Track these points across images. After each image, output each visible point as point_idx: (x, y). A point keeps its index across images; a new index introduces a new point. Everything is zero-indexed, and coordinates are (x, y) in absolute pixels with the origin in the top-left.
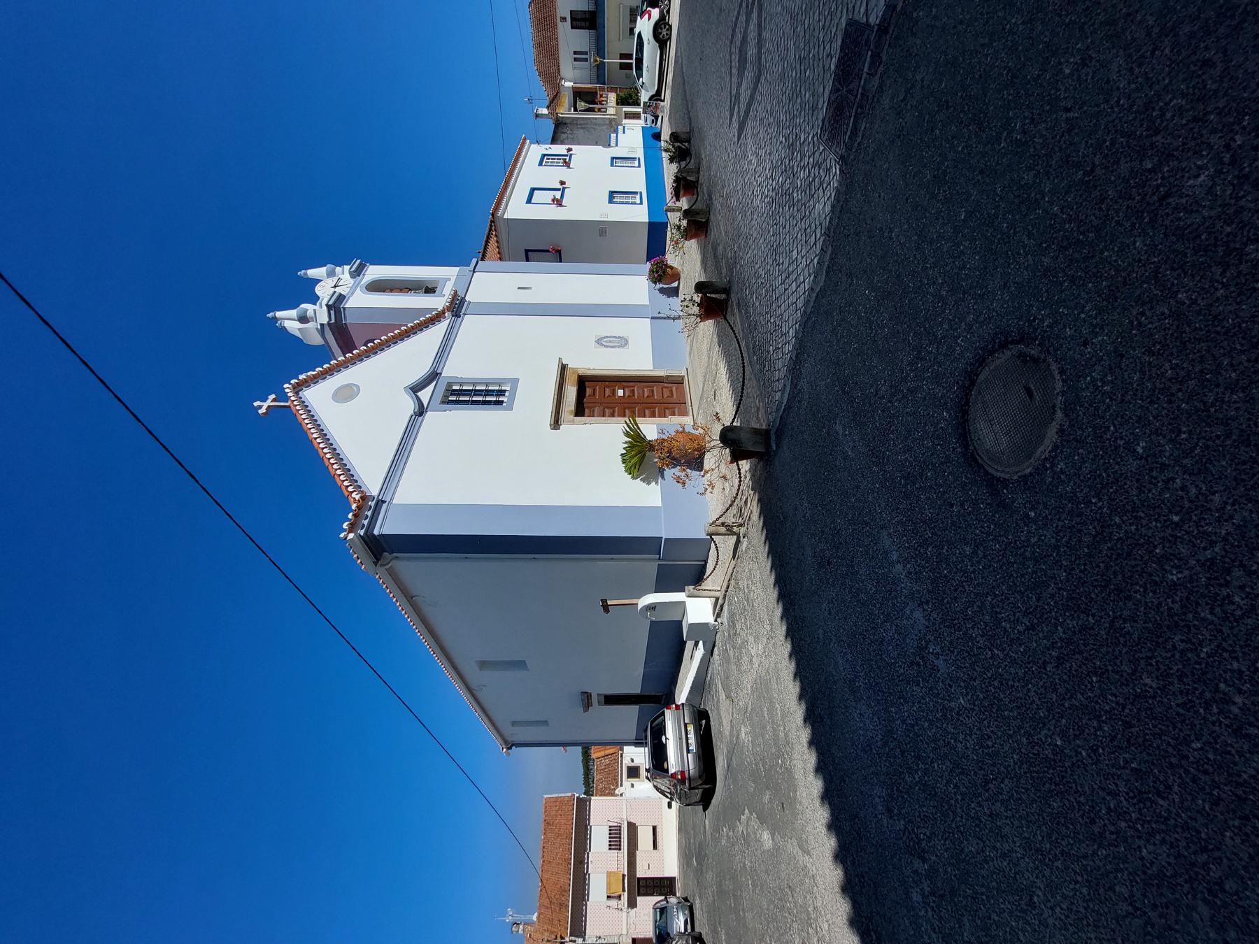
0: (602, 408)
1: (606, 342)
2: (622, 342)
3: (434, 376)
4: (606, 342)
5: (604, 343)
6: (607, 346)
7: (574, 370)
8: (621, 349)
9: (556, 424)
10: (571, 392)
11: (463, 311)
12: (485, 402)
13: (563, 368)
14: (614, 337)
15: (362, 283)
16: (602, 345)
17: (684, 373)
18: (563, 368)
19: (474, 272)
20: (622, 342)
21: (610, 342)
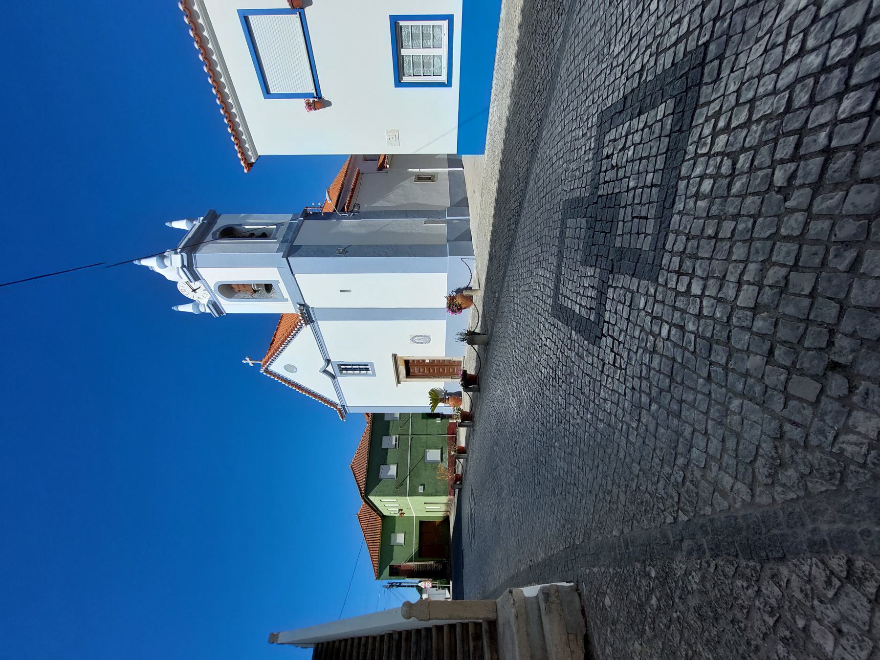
2: (427, 339)
3: (328, 361)
6: (418, 343)
7: (401, 358)
8: (427, 344)
9: (399, 382)
10: (402, 369)
11: (314, 319)
12: (359, 365)
13: (395, 356)
14: (422, 336)
15: (213, 290)
16: (414, 342)
17: (462, 359)
18: (395, 356)
20: (427, 339)
21: (420, 339)
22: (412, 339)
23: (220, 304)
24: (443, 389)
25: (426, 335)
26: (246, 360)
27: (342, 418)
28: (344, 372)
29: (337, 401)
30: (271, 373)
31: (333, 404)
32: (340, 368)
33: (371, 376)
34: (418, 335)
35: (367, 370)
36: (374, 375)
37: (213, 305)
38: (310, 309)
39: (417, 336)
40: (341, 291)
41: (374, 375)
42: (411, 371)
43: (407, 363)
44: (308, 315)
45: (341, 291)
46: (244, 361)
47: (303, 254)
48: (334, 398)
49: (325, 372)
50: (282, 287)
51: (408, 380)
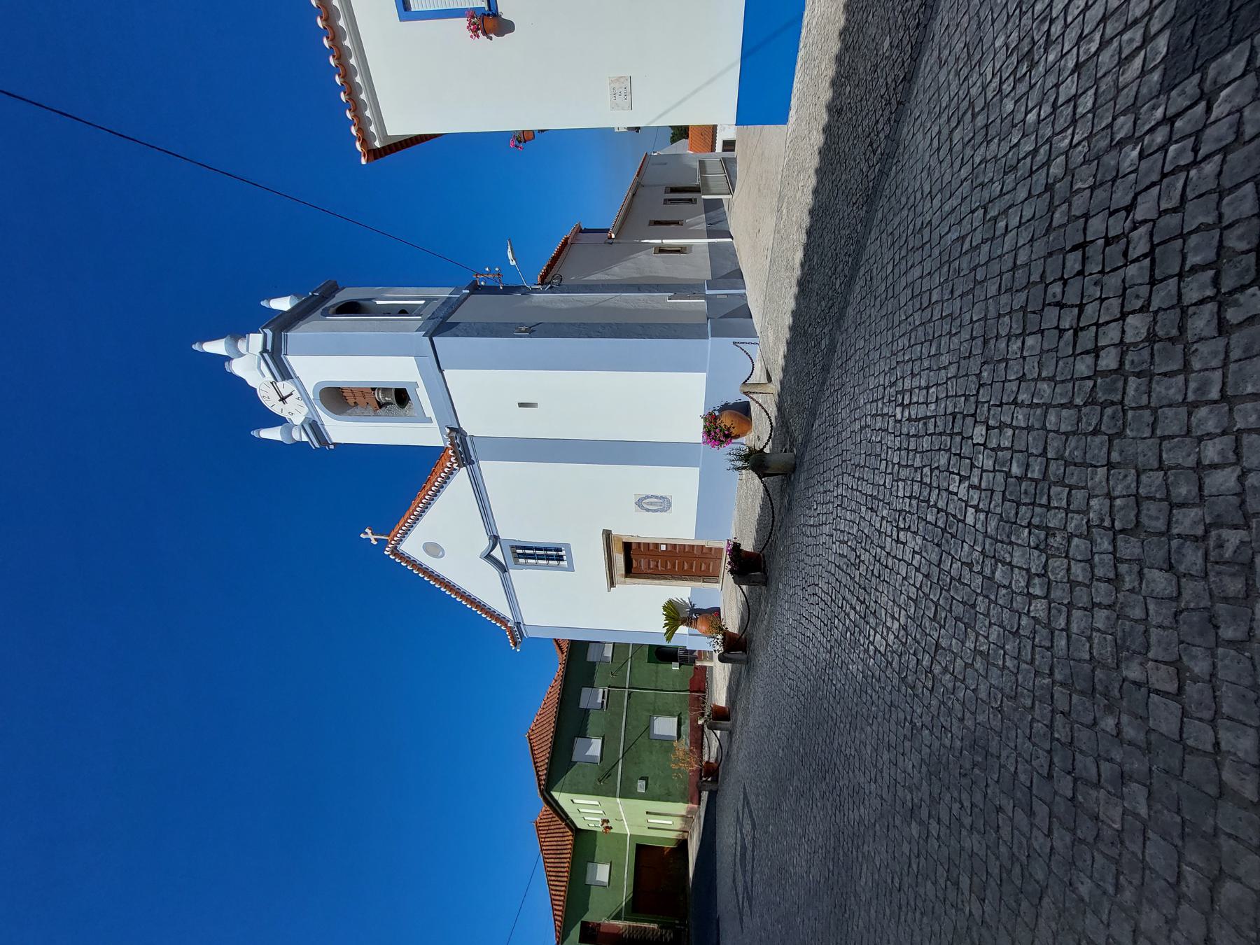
0: (647, 560)
1: (647, 503)
2: (663, 504)
3: (495, 539)
4: (647, 503)
5: (645, 506)
6: (648, 510)
7: (619, 538)
9: (612, 584)
10: (619, 560)
11: (473, 458)
12: (546, 549)
13: (607, 535)
14: (656, 497)
15: (312, 397)
16: (642, 508)
18: (607, 535)
19: (441, 371)
20: (663, 504)
21: (651, 504)
22: (639, 503)
23: (323, 425)
24: (687, 601)
25: (661, 495)
26: (366, 533)
27: (515, 644)
28: (521, 560)
29: (509, 615)
30: (402, 556)
31: (503, 620)
32: (514, 553)
33: (563, 569)
34: (650, 494)
35: (560, 558)
36: (571, 568)
37: (310, 425)
38: (468, 439)
39: (647, 497)
40: (521, 405)
41: (571, 568)
42: (634, 563)
43: (627, 547)
44: (463, 448)
45: (521, 405)
46: (362, 536)
47: (457, 333)
48: (502, 608)
49: (488, 557)
50: (422, 397)
51: (628, 580)
